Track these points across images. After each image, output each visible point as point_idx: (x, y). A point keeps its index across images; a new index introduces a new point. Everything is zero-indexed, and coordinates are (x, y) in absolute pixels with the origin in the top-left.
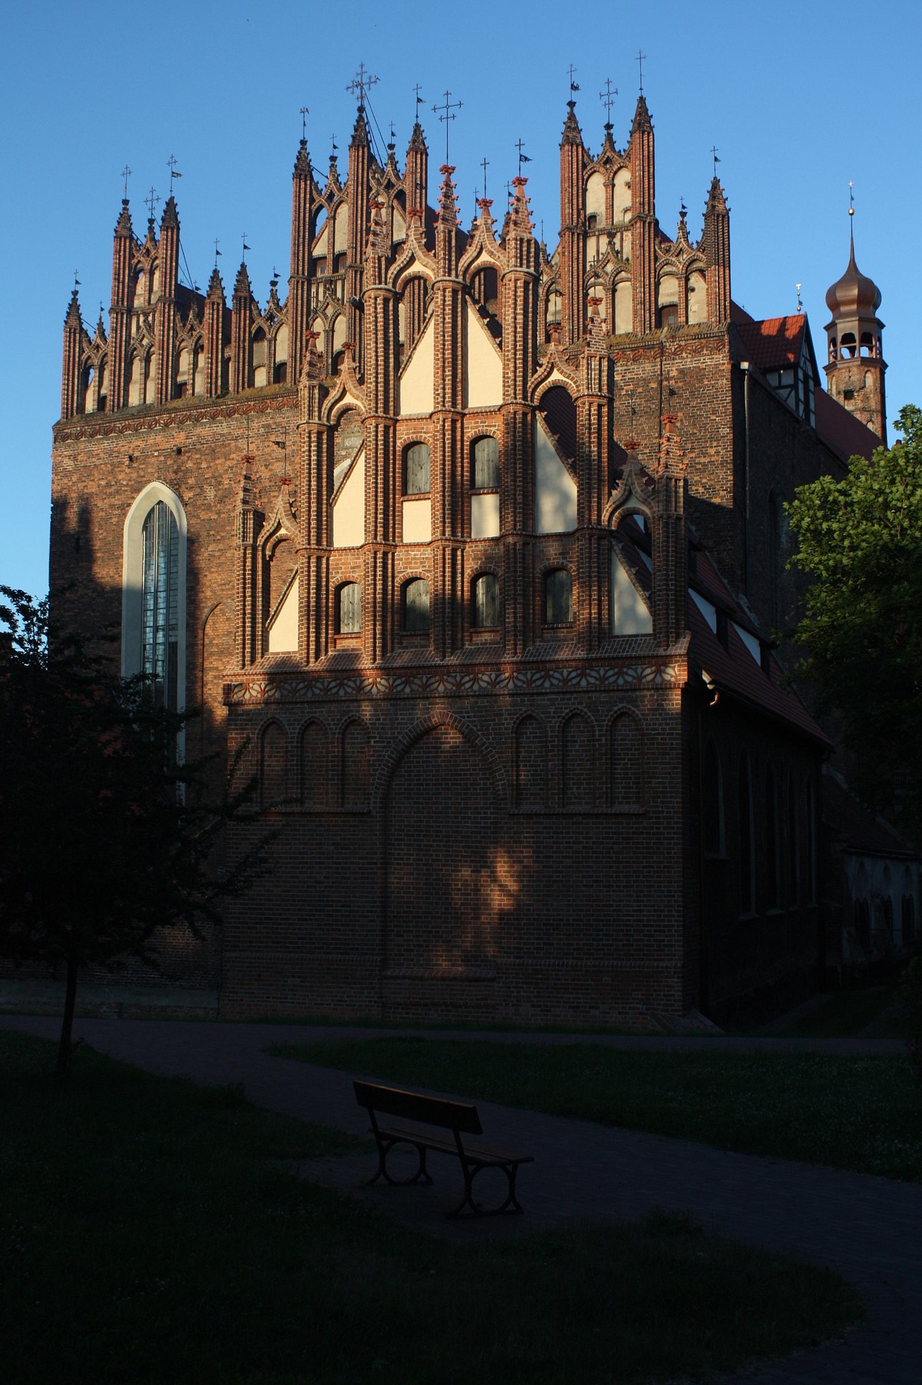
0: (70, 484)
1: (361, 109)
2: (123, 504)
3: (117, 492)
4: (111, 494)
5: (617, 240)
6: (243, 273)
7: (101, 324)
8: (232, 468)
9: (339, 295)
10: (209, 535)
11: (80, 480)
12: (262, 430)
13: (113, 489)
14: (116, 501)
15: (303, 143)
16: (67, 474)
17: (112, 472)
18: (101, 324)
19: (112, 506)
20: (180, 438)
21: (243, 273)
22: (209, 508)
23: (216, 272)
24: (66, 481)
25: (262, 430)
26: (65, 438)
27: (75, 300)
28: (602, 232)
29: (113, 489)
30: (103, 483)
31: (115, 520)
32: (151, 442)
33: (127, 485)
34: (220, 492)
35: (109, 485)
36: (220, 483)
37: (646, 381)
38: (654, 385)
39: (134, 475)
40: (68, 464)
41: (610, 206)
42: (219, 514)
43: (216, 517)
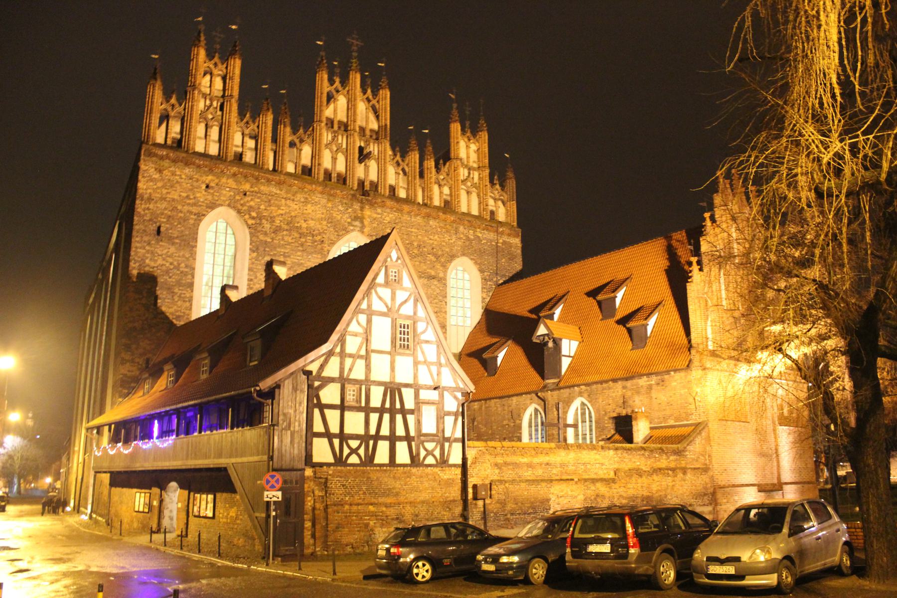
0: (155, 187)
2: (199, 213)
4: (189, 204)
8: (282, 215)
9: (340, 141)
10: (264, 250)
11: (163, 187)
12: (302, 200)
13: (191, 201)
14: (194, 209)
17: (191, 190)
19: (191, 213)
20: (247, 187)
22: (266, 234)
24: (151, 184)
25: (302, 200)
28: (466, 166)
29: (191, 201)
30: (184, 195)
31: (192, 222)
33: (203, 202)
34: (274, 227)
35: (188, 197)
36: (274, 221)
37: (491, 241)
38: (494, 243)
41: (468, 157)
42: (273, 239)
43: (270, 240)
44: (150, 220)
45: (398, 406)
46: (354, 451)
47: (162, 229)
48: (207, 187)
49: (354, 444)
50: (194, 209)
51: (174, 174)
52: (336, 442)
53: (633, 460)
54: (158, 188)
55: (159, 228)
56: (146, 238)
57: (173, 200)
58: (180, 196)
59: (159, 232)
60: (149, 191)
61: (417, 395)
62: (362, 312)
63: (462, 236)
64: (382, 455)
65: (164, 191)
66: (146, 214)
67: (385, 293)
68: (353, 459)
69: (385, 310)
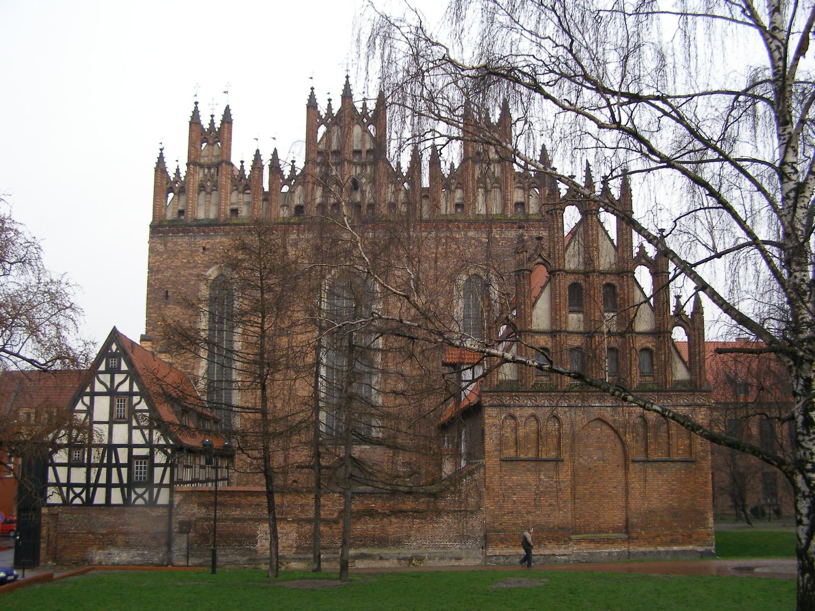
1: (347, 77)
3: (195, 267)
4: (190, 268)
5: (492, 167)
6: (275, 153)
7: (178, 170)
11: (168, 258)
13: (191, 265)
14: (194, 272)
15: (312, 89)
16: (160, 254)
18: (178, 170)
19: (191, 274)
21: (275, 153)
23: (258, 151)
24: (158, 257)
26: (159, 232)
27: (161, 154)
29: (191, 265)
31: (192, 282)
32: (217, 240)
35: (188, 262)
39: (206, 259)
40: (161, 248)
44: (160, 288)
45: (114, 461)
46: (78, 495)
47: (169, 294)
48: (204, 249)
49: (78, 490)
50: (194, 272)
51: (176, 244)
52: (64, 489)
53: (366, 502)
54: (164, 259)
55: (167, 292)
56: (157, 304)
57: (177, 267)
58: (182, 262)
59: (167, 297)
60: (158, 263)
61: (130, 453)
62: (87, 394)
63: (473, 241)
64: (100, 497)
65: (169, 261)
66: (156, 283)
67: (106, 378)
68: (78, 501)
69: (105, 390)
